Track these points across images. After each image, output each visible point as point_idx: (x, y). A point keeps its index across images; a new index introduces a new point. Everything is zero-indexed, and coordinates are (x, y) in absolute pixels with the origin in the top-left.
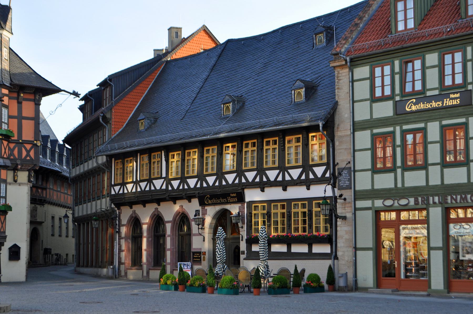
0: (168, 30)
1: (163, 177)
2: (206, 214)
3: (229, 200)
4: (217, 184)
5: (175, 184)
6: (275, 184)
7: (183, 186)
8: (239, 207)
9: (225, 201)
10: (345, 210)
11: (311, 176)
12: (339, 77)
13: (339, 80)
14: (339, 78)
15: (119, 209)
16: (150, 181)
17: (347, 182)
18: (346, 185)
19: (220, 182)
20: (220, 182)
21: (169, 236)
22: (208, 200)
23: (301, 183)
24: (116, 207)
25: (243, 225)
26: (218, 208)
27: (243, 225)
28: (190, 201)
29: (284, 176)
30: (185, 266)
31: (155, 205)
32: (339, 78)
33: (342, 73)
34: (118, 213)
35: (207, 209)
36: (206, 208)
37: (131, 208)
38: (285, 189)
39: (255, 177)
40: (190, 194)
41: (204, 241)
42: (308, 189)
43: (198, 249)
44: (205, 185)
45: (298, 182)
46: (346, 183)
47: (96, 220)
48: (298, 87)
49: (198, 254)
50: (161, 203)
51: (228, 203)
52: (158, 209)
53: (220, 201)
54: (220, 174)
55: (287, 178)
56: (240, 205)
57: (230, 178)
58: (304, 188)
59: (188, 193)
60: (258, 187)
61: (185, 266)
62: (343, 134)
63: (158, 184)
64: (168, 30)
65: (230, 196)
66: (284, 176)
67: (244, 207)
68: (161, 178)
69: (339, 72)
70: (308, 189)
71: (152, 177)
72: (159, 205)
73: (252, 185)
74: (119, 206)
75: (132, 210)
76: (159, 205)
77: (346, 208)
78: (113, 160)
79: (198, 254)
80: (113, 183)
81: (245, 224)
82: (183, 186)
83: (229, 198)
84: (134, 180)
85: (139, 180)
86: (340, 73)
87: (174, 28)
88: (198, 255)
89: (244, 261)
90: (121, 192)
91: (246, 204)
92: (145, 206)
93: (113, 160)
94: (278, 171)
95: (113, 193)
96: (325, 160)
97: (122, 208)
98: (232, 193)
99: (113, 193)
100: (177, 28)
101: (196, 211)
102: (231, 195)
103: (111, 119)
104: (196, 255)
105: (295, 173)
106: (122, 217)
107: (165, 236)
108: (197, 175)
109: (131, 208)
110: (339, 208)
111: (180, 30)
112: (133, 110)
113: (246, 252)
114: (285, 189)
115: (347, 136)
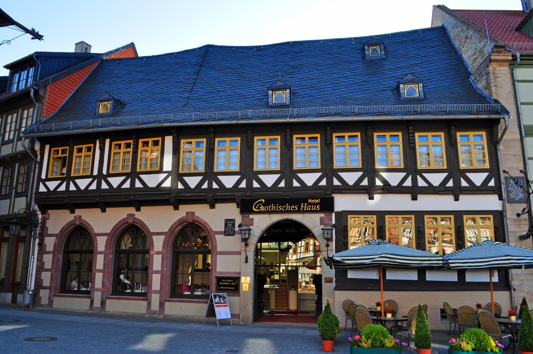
0: (76, 44)
1: (164, 170)
2: (252, 225)
3: (303, 208)
4: (282, 184)
5: (193, 182)
6: (400, 189)
7: (210, 184)
8: (321, 218)
10: (520, 228)
11: (464, 183)
12: (496, 74)
13: (495, 77)
14: (495, 75)
15: (43, 213)
16: (134, 175)
17: (520, 195)
18: (519, 198)
19: (289, 183)
20: (289, 183)
21: (158, 253)
22: (260, 206)
23: (446, 191)
24: (40, 210)
25: (329, 243)
26: (276, 218)
27: (329, 243)
28: (212, 207)
29: (414, 181)
30: (221, 299)
31: (131, 210)
32: (495, 75)
33: (499, 70)
34: (40, 216)
35: (253, 219)
36: (251, 216)
37: (72, 212)
38: (414, 198)
39: (361, 179)
40: (219, 196)
41: (246, 261)
42: (457, 199)
43: (228, 272)
44: (256, 185)
45: (441, 189)
46: (519, 196)
47: (16, 224)
48: (411, 81)
49: (230, 281)
50: (142, 208)
51: (299, 211)
52: (134, 215)
53: (285, 208)
54: (287, 171)
55: (421, 183)
56: (323, 215)
57: (309, 179)
58: (451, 198)
59: (218, 194)
60: (365, 193)
61: (221, 299)
62: (510, 137)
63: (152, 181)
64: (76, 44)
65: (307, 202)
66: (414, 181)
67: (332, 218)
68: (160, 171)
69: (495, 68)
70: (457, 199)
71: (138, 170)
72: (138, 210)
73: (356, 189)
74: (44, 209)
75: (73, 215)
76: (138, 210)
77: (522, 226)
78: (47, 147)
79: (230, 281)
80: (43, 176)
81: (332, 241)
82: (210, 184)
83: (304, 205)
84: (95, 173)
85: (105, 172)
86: (497, 70)
87: (85, 43)
88: (230, 282)
89: (336, 291)
90: (63, 188)
91: (334, 215)
92: (104, 211)
93: (47, 147)
94: (404, 174)
95: (42, 189)
96: (487, 166)
97: (50, 211)
98: (313, 199)
99: (42, 189)
100: (87, 44)
101: (227, 220)
102: (310, 201)
103: (43, 98)
104: (225, 282)
105: (436, 179)
106: (49, 224)
107: (147, 252)
108: (240, 172)
109: (72, 212)
110: (512, 225)
111: (89, 47)
112: (67, 97)
113: (334, 279)
114: (414, 198)
115: (515, 140)
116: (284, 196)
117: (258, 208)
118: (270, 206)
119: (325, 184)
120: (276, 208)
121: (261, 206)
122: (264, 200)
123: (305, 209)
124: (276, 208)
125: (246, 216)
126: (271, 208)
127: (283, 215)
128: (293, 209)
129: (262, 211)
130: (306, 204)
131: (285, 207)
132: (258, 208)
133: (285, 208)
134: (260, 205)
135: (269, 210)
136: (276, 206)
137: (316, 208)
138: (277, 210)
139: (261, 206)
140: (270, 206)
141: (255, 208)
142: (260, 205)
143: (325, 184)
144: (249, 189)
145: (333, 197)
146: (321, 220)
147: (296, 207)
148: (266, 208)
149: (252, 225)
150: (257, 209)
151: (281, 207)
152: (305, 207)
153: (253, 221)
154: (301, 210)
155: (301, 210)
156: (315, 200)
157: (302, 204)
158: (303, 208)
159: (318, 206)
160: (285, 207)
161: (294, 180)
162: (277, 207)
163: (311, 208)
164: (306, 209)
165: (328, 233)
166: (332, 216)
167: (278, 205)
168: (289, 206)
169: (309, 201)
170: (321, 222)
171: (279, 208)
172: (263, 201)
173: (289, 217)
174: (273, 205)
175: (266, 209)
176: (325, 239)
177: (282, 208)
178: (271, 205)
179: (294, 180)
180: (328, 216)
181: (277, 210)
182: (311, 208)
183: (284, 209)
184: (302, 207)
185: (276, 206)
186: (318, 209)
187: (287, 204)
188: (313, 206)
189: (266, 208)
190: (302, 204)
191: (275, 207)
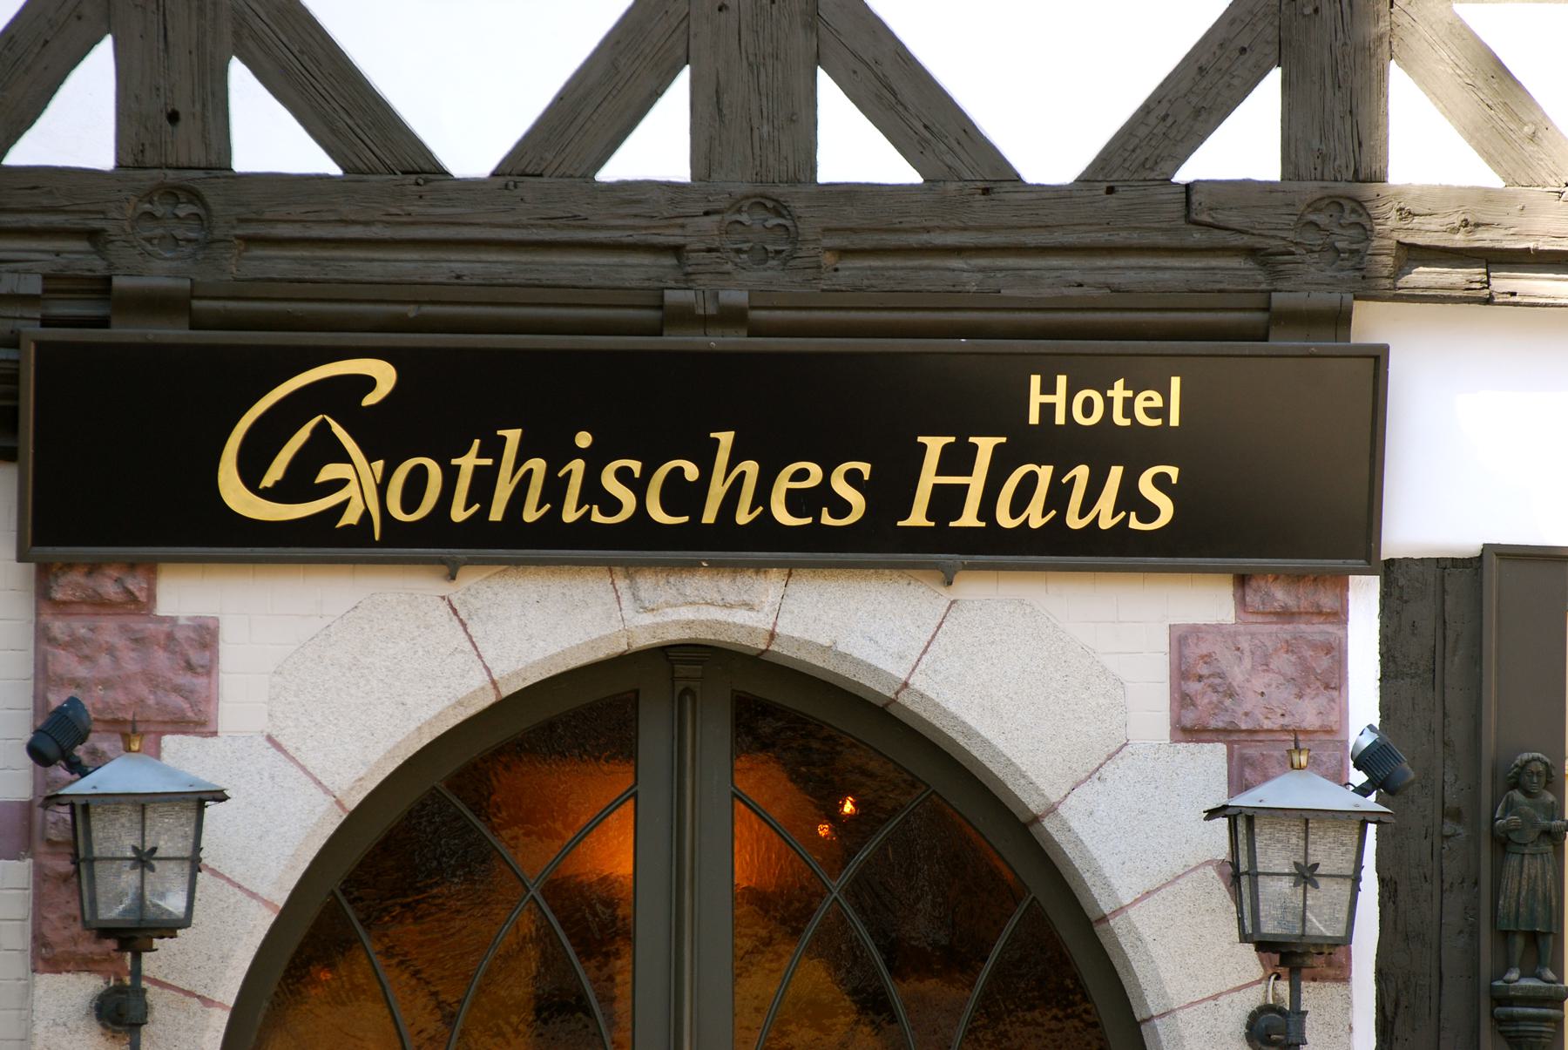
2: (197, 724)
3: (947, 501)
8: (1182, 639)
9: (824, 496)
22: (324, 449)
35: (206, 635)
53: (682, 496)
67: (1336, 653)
116: (685, 318)
117: (297, 486)
118: (468, 463)
119: (1270, 170)
120: (554, 491)
121: (345, 458)
122: (384, 375)
123: (969, 518)
124: (554, 491)
125: (108, 587)
126: (484, 483)
127: (650, 586)
128: (795, 502)
129: (351, 517)
130: (986, 446)
131: (691, 472)
132: (297, 486)
133: (682, 496)
134: (323, 430)
135: (459, 514)
136: (559, 454)
137: (1129, 499)
138: (570, 515)
139: (345, 458)
140: (468, 463)
141: (251, 474)
142: (323, 430)
143: (1270, 170)
144: (172, 193)
145: (1377, 358)
146: (1182, 673)
147: (841, 487)
148: (418, 479)
149: (197, 724)
150: (279, 493)
151: (624, 476)
152: (976, 483)
153: (209, 670)
154: (918, 517)
155: (918, 517)
156: (1119, 392)
157: (934, 445)
158: (947, 501)
159: (1161, 482)
160: (691, 472)
161: (827, 89)
162: (577, 467)
163: (1058, 496)
164: (987, 509)
165: (1306, 875)
166: (1339, 616)
167: (584, 440)
168: (751, 468)
169: (1036, 398)
170: (1182, 700)
171: (593, 492)
172: (368, 383)
173: (741, 617)
174: (513, 436)
175: (412, 498)
176: (1264, 946)
177: (639, 487)
178: (494, 448)
179: (827, 89)
180: (1285, 615)
181: (570, 515)
182: (1058, 496)
183: (668, 508)
184: (928, 479)
185: (559, 454)
186: (1150, 512)
187: (726, 439)
188: (1082, 473)
189: (418, 479)
190: (934, 445)
191: (538, 465)
